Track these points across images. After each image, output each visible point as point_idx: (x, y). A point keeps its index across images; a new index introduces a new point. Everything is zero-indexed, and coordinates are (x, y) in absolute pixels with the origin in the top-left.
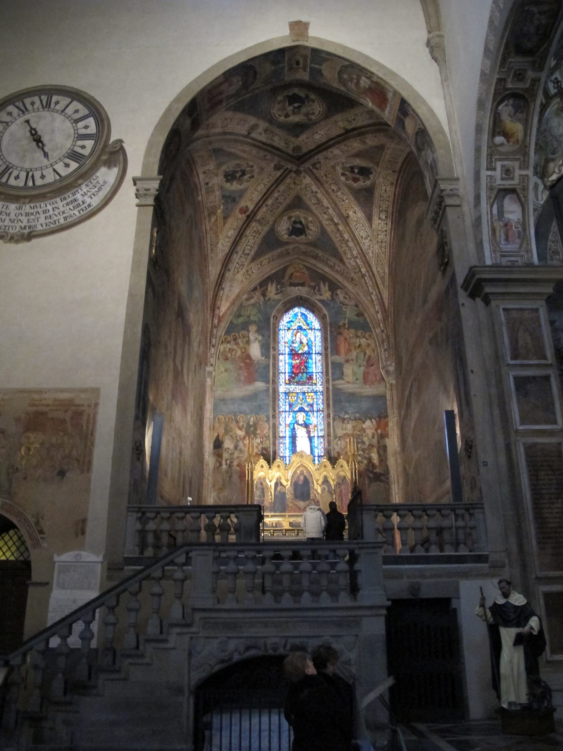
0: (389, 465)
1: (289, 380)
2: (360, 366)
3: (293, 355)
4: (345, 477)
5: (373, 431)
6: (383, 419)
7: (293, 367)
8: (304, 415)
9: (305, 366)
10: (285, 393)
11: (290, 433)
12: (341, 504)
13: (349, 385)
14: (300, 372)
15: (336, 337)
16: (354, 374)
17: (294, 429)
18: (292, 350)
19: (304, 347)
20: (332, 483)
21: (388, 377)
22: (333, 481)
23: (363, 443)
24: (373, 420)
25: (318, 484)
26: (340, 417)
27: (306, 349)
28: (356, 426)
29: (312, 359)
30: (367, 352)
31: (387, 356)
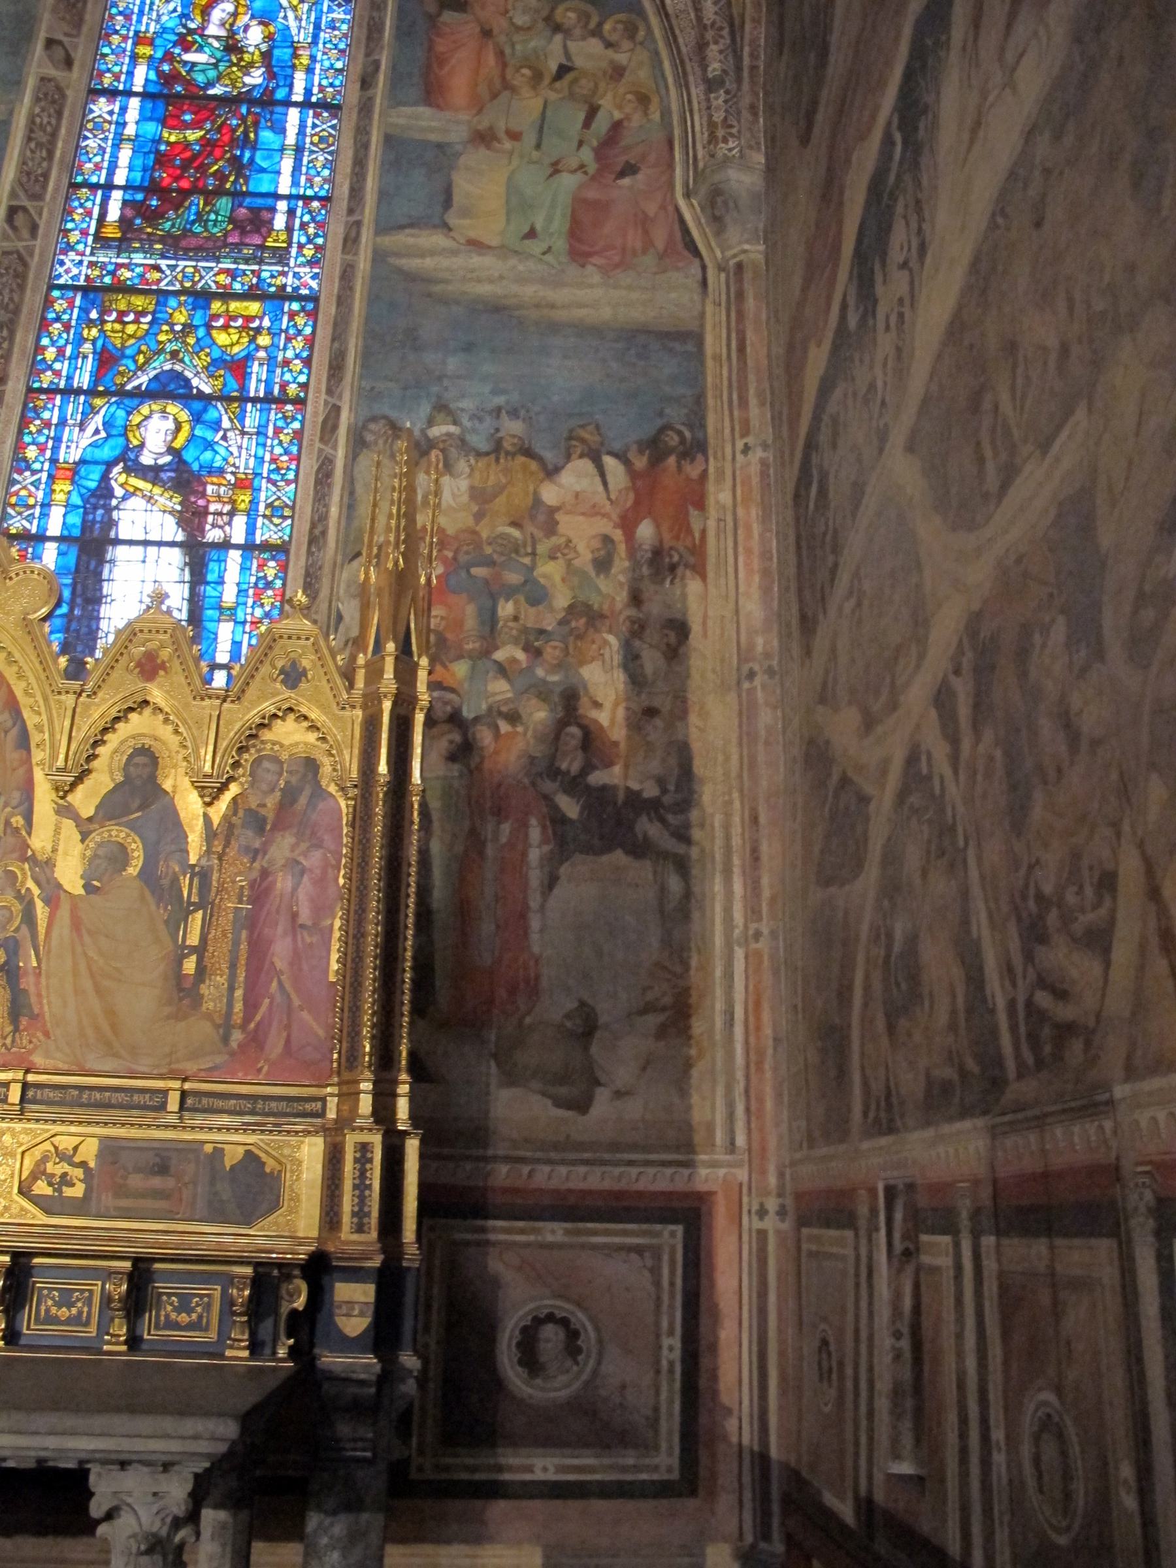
0: (696, 746)
1: (124, 222)
2: (556, 169)
3: (170, 99)
4: (311, 765)
5: (604, 526)
6: (672, 460)
7: (162, 160)
8: (184, 416)
9: (236, 162)
10: (88, 289)
11: (75, 519)
12: (251, 1006)
13: (476, 260)
14: (195, 190)
15: (432, 19)
16: (517, 203)
17: (104, 491)
18: (168, 79)
19: (247, 69)
20: (190, 805)
21: (719, 232)
22: (210, 795)
23: (537, 596)
24: (609, 461)
25: (65, 811)
26: (395, 429)
27: (256, 78)
28: (500, 489)
29: (283, 131)
30: (606, 102)
31: (718, 117)
